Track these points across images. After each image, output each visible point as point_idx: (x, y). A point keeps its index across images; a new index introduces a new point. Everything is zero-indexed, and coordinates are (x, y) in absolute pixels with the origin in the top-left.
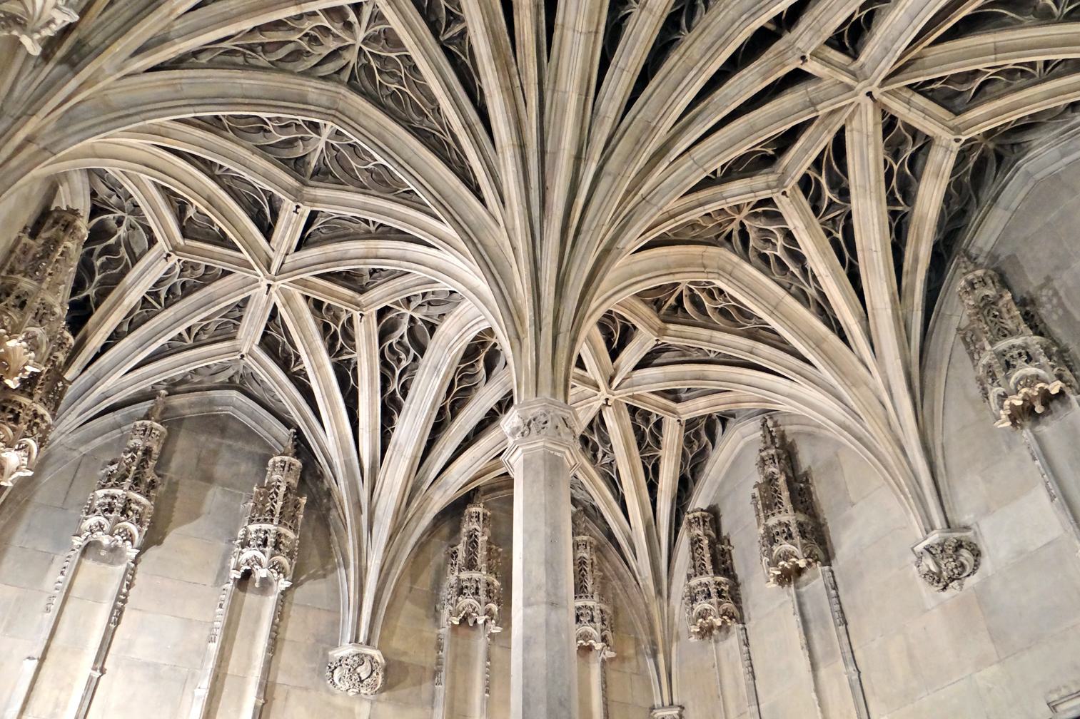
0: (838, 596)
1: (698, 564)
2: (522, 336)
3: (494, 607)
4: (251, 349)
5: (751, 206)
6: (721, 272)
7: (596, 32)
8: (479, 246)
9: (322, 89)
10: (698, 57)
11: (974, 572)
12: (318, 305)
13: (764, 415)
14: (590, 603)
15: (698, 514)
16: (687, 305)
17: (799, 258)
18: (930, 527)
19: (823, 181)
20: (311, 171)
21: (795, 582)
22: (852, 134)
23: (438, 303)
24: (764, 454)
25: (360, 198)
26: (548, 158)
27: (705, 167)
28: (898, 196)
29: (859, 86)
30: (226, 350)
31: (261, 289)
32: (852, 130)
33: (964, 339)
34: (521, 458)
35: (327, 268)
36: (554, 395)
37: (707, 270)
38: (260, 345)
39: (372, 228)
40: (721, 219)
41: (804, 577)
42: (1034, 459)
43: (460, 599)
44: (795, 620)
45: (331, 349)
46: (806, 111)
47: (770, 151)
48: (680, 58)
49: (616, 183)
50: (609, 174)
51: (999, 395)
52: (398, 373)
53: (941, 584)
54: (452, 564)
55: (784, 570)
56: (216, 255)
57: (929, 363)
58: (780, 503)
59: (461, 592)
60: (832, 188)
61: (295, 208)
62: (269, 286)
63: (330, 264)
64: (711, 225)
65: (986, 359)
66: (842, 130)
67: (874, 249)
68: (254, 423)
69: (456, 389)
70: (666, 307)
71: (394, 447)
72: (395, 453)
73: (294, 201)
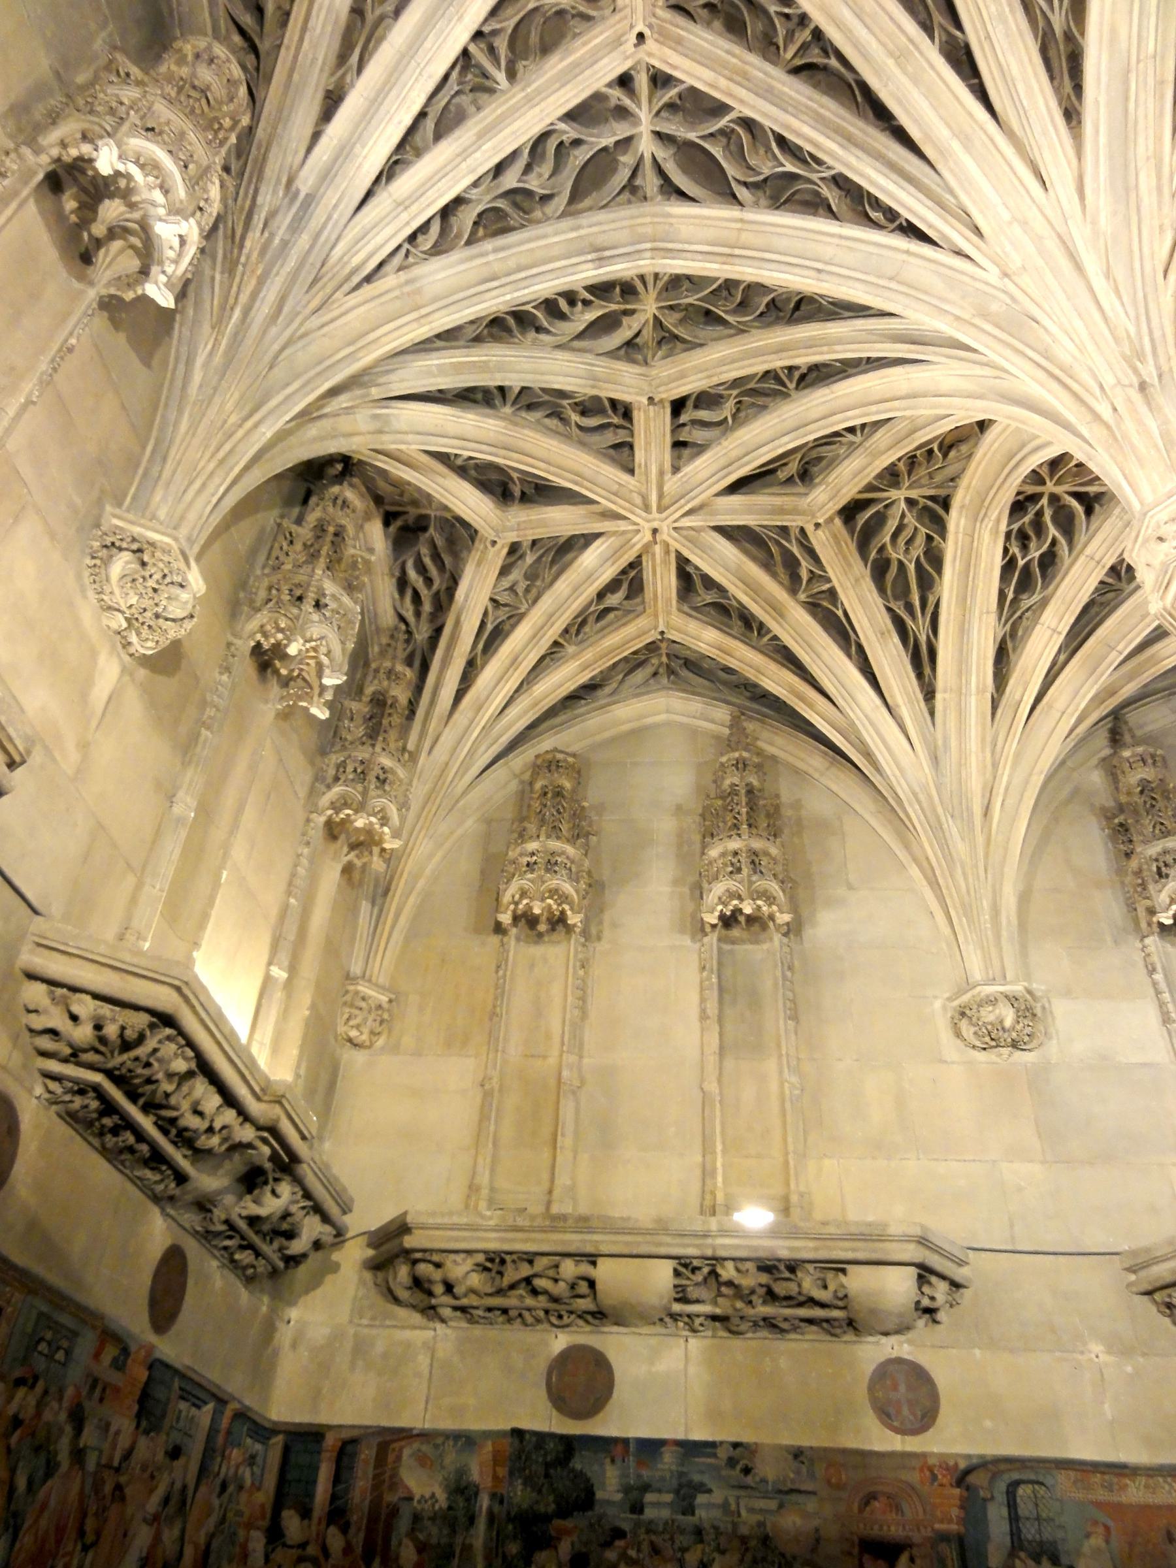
67: (1120, 648)
71: (408, 282)
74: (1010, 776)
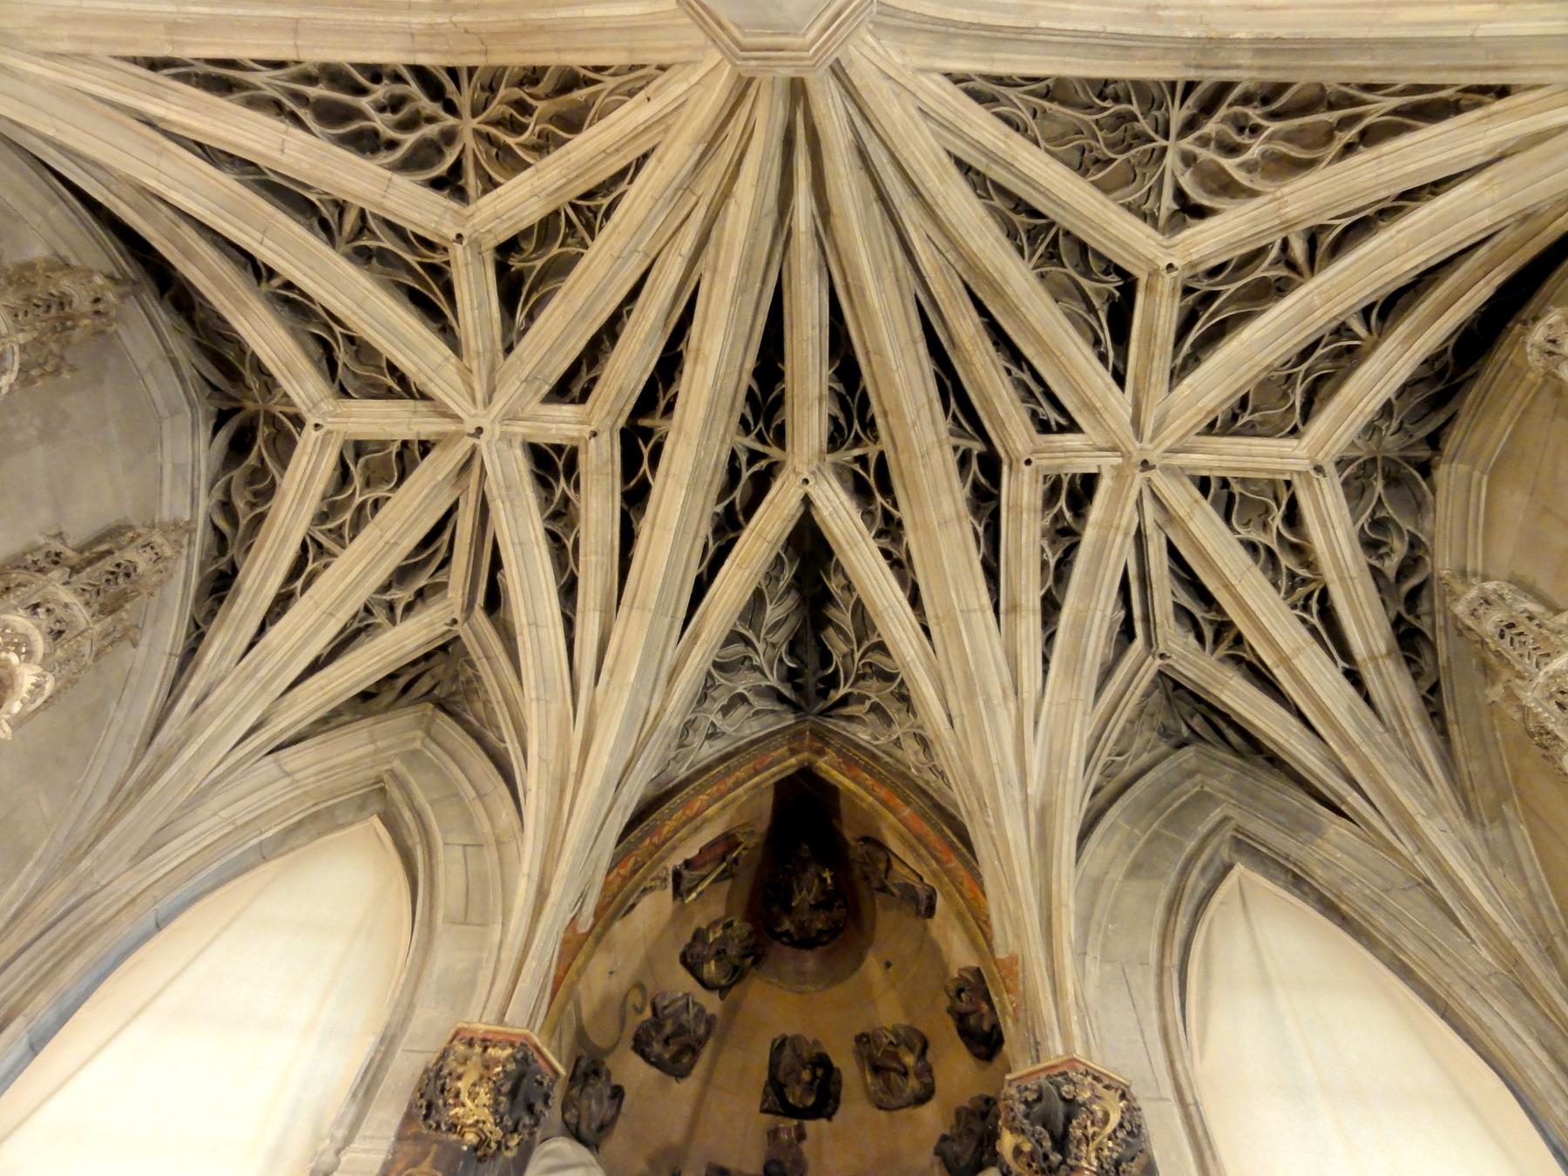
7: (867, 354)
9: (1228, 68)
17: (330, 114)
19: (410, 259)
26: (872, 194)
29: (497, 431)
32: (447, 359)
40: (496, 109)
47: (516, 263)
48: (742, 366)
67: (267, 241)
74: (36, 82)
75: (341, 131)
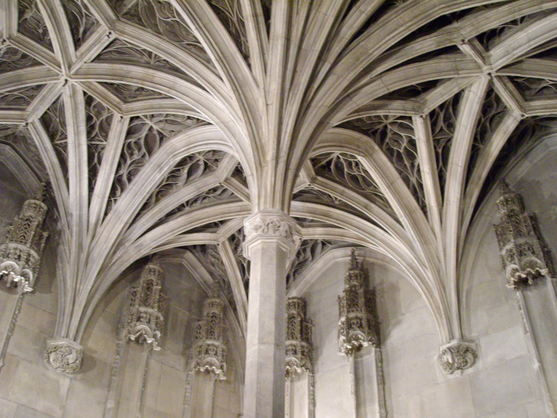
0: (382, 367)
1: (290, 332)
2: (263, 164)
3: (159, 334)
4: (33, 121)
5: (395, 117)
6: (366, 153)
8: (242, 96)
10: (407, 20)
11: (471, 367)
12: (89, 101)
13: (353, 248)
14: (216, 343)
15: (295, 300)
16: (332, 167)
17: (412, 156)
18: (452, 337)
19: (442, 115)
20: (125, 11)
21: (355, 354)
22: (469, 94)
23: (173, 122)
24: (351, 272)
25: (155, 40)
27: (389, 87)
28: (478, 137)
30: (16, 116)
31: (60, 81)
32: (470, 91)
33: (496, 231)
34: (260, 247)
35: (113, 80)
36: (282, 209)
37: (360, 150)
38: (40, 119)
39: (152, 62)
41: (363, 352)
42: (520, 309)
43: (138, 323)
44: (349, 378)
45: (89, 133)
46: (453, 72)
47: (420, 88)
49: (339, 82)
50: (335, 74)
51: (513, 269)
52: (129, 162)
53: (451, 371)
54: (132, 300)
55: (353, 346)
56: (35, 49)
57: (469, 240)
58: (357, 305)
59: (139, 319)
60: (444, 121)
61: (107, 34)
62: (66, 81)
63: (115, 77)
64: (369, 122)
65: (510, 246)
66: (463, 90)
67: (460, 164)
68: (17, 172)
69: (164, 183)
70: (319, 165)
72: (114, 217)
73: (109, 28)
75: (415, 153)
